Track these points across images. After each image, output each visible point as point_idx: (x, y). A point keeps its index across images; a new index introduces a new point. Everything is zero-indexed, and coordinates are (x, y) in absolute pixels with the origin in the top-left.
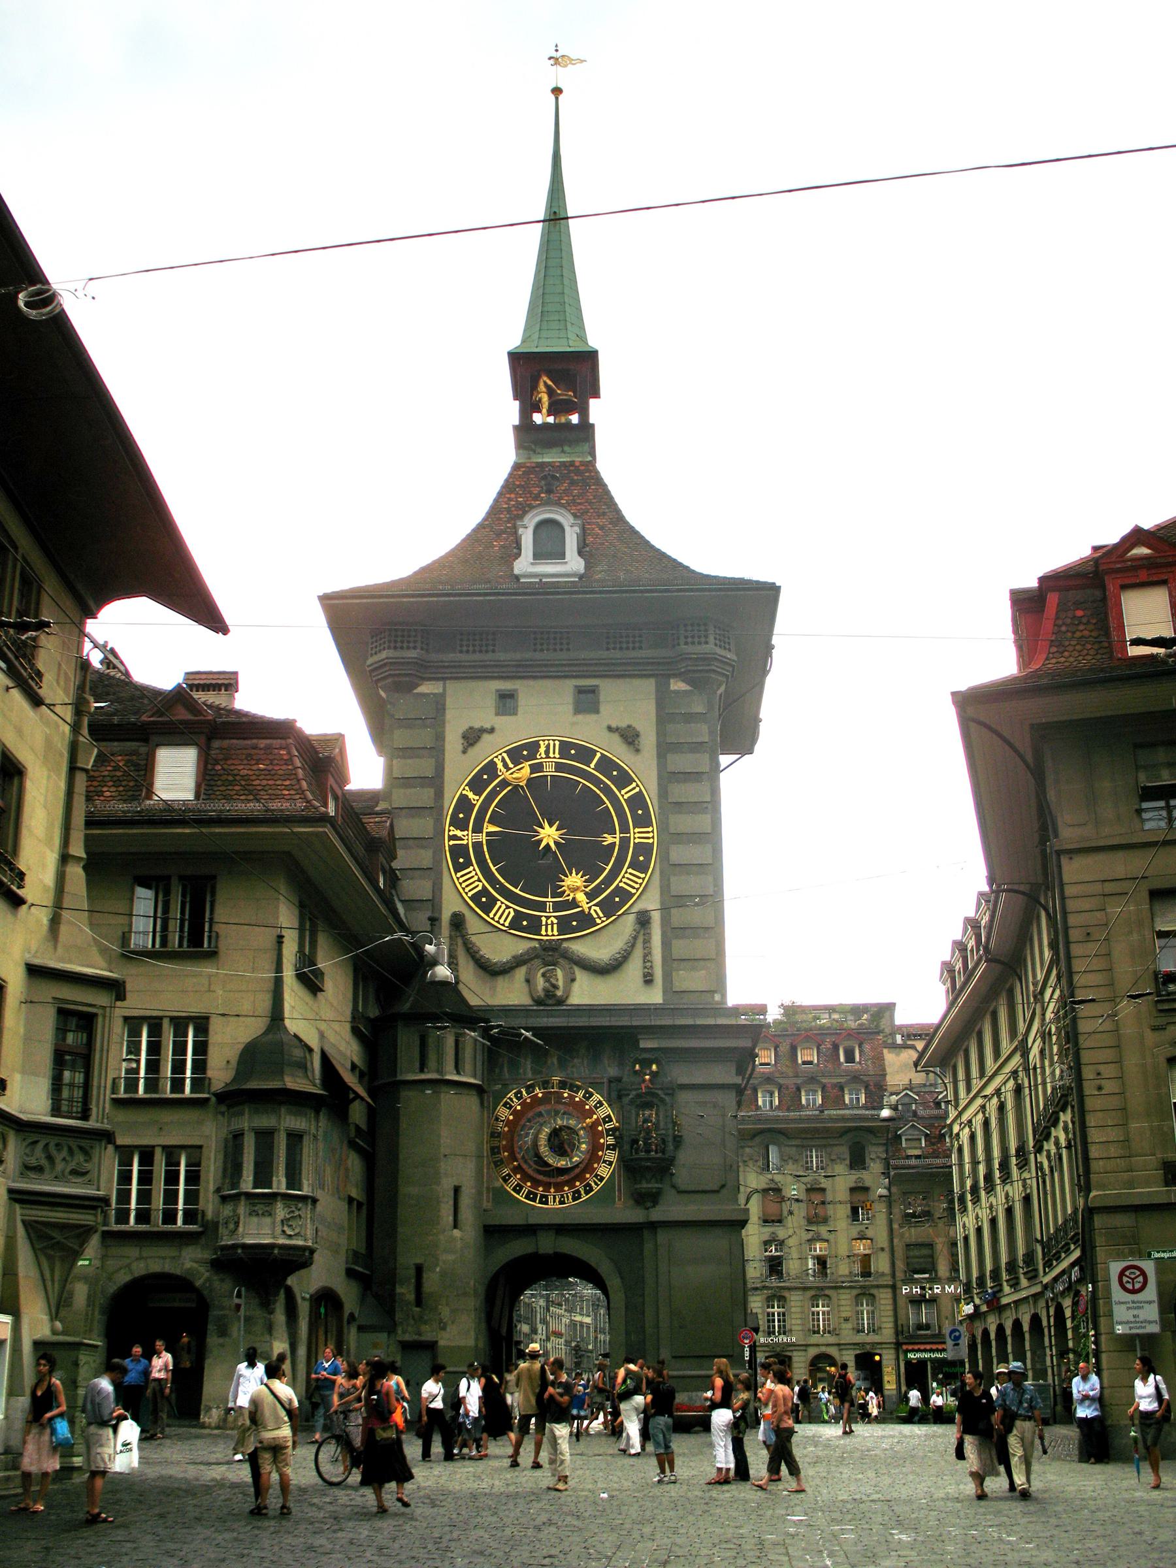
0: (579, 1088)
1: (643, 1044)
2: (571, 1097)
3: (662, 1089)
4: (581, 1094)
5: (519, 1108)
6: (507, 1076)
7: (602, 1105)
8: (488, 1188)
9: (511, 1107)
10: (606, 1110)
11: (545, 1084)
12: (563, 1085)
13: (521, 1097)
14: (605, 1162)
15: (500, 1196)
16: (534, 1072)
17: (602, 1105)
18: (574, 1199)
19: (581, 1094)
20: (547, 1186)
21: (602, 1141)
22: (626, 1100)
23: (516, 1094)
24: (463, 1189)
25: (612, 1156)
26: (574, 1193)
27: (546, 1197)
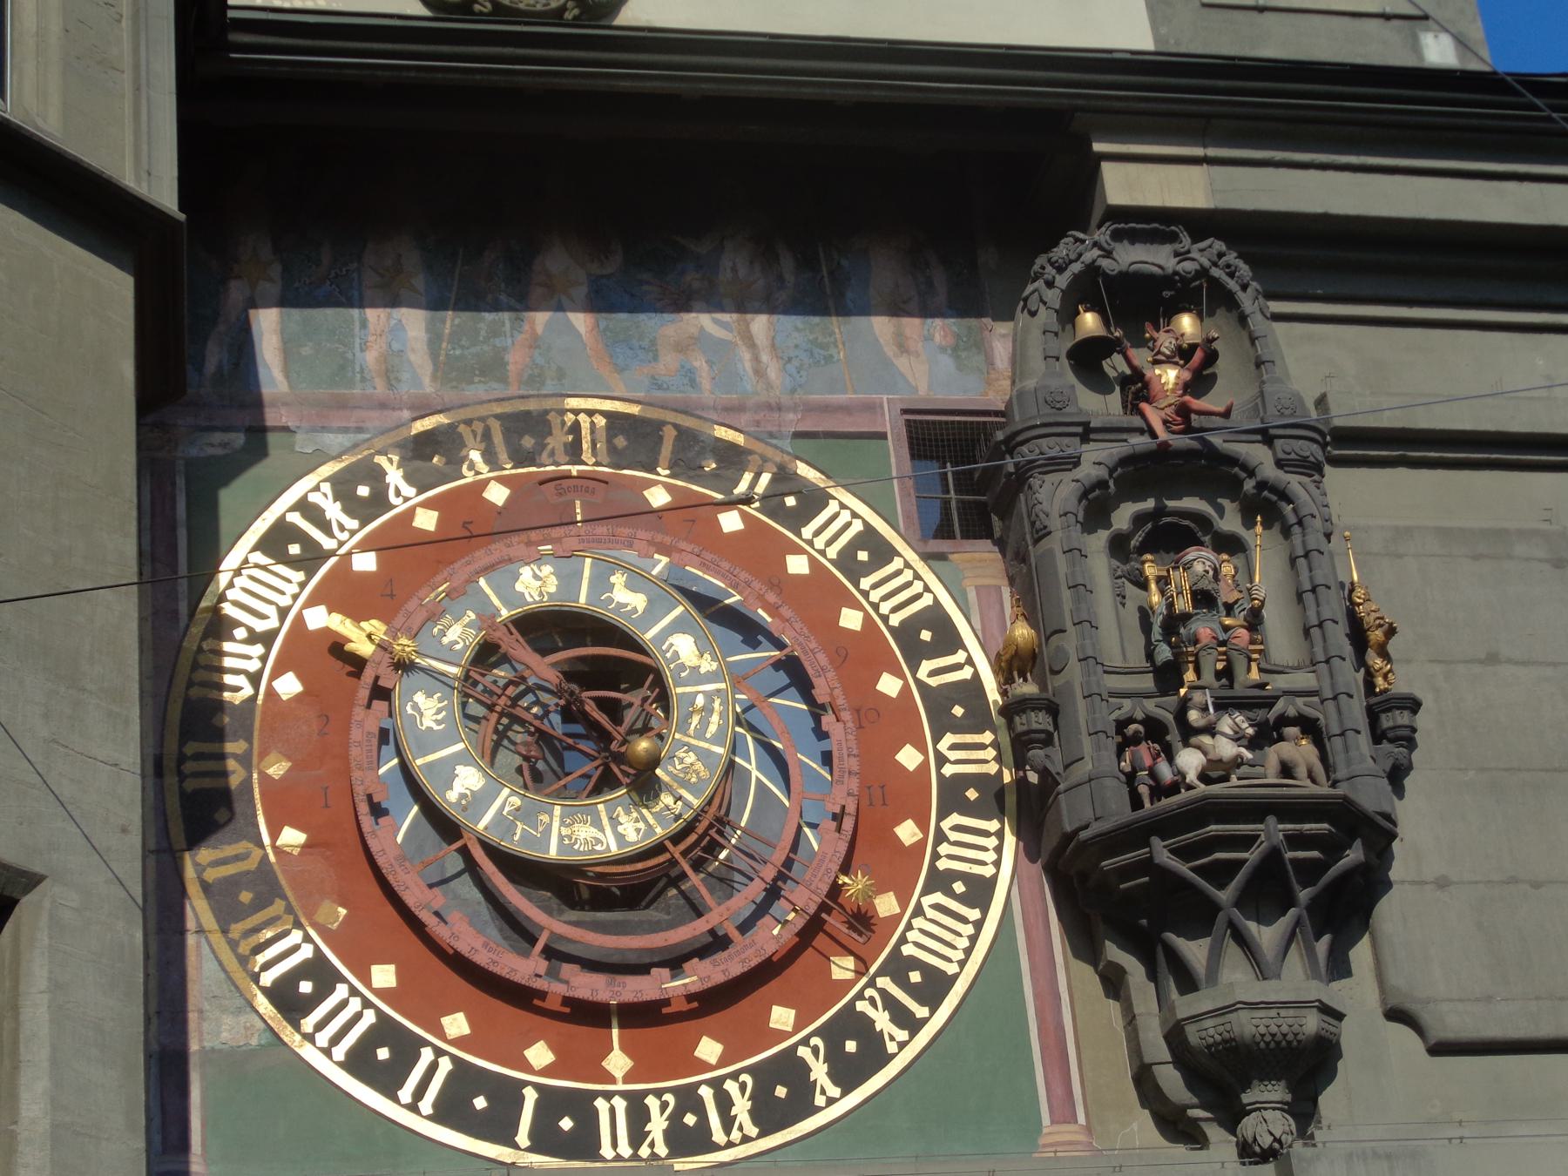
0: (733, 459)
1: (1129, 182)
2: (690, 517)
3: (1267, 438)
5: (366, 562)
7: (883, 553)
9: (312, 558)
10: (910, 583)
11: (525, 432)
12: (635, 439)
13: (379, 501)
14: (941, 880)
17: (883, 553)
18: (769, 1116)
21: (909, 757)
22: (1055, 496)
23: (342, 488)
26: (765, 1076)
27: (582, 1106)
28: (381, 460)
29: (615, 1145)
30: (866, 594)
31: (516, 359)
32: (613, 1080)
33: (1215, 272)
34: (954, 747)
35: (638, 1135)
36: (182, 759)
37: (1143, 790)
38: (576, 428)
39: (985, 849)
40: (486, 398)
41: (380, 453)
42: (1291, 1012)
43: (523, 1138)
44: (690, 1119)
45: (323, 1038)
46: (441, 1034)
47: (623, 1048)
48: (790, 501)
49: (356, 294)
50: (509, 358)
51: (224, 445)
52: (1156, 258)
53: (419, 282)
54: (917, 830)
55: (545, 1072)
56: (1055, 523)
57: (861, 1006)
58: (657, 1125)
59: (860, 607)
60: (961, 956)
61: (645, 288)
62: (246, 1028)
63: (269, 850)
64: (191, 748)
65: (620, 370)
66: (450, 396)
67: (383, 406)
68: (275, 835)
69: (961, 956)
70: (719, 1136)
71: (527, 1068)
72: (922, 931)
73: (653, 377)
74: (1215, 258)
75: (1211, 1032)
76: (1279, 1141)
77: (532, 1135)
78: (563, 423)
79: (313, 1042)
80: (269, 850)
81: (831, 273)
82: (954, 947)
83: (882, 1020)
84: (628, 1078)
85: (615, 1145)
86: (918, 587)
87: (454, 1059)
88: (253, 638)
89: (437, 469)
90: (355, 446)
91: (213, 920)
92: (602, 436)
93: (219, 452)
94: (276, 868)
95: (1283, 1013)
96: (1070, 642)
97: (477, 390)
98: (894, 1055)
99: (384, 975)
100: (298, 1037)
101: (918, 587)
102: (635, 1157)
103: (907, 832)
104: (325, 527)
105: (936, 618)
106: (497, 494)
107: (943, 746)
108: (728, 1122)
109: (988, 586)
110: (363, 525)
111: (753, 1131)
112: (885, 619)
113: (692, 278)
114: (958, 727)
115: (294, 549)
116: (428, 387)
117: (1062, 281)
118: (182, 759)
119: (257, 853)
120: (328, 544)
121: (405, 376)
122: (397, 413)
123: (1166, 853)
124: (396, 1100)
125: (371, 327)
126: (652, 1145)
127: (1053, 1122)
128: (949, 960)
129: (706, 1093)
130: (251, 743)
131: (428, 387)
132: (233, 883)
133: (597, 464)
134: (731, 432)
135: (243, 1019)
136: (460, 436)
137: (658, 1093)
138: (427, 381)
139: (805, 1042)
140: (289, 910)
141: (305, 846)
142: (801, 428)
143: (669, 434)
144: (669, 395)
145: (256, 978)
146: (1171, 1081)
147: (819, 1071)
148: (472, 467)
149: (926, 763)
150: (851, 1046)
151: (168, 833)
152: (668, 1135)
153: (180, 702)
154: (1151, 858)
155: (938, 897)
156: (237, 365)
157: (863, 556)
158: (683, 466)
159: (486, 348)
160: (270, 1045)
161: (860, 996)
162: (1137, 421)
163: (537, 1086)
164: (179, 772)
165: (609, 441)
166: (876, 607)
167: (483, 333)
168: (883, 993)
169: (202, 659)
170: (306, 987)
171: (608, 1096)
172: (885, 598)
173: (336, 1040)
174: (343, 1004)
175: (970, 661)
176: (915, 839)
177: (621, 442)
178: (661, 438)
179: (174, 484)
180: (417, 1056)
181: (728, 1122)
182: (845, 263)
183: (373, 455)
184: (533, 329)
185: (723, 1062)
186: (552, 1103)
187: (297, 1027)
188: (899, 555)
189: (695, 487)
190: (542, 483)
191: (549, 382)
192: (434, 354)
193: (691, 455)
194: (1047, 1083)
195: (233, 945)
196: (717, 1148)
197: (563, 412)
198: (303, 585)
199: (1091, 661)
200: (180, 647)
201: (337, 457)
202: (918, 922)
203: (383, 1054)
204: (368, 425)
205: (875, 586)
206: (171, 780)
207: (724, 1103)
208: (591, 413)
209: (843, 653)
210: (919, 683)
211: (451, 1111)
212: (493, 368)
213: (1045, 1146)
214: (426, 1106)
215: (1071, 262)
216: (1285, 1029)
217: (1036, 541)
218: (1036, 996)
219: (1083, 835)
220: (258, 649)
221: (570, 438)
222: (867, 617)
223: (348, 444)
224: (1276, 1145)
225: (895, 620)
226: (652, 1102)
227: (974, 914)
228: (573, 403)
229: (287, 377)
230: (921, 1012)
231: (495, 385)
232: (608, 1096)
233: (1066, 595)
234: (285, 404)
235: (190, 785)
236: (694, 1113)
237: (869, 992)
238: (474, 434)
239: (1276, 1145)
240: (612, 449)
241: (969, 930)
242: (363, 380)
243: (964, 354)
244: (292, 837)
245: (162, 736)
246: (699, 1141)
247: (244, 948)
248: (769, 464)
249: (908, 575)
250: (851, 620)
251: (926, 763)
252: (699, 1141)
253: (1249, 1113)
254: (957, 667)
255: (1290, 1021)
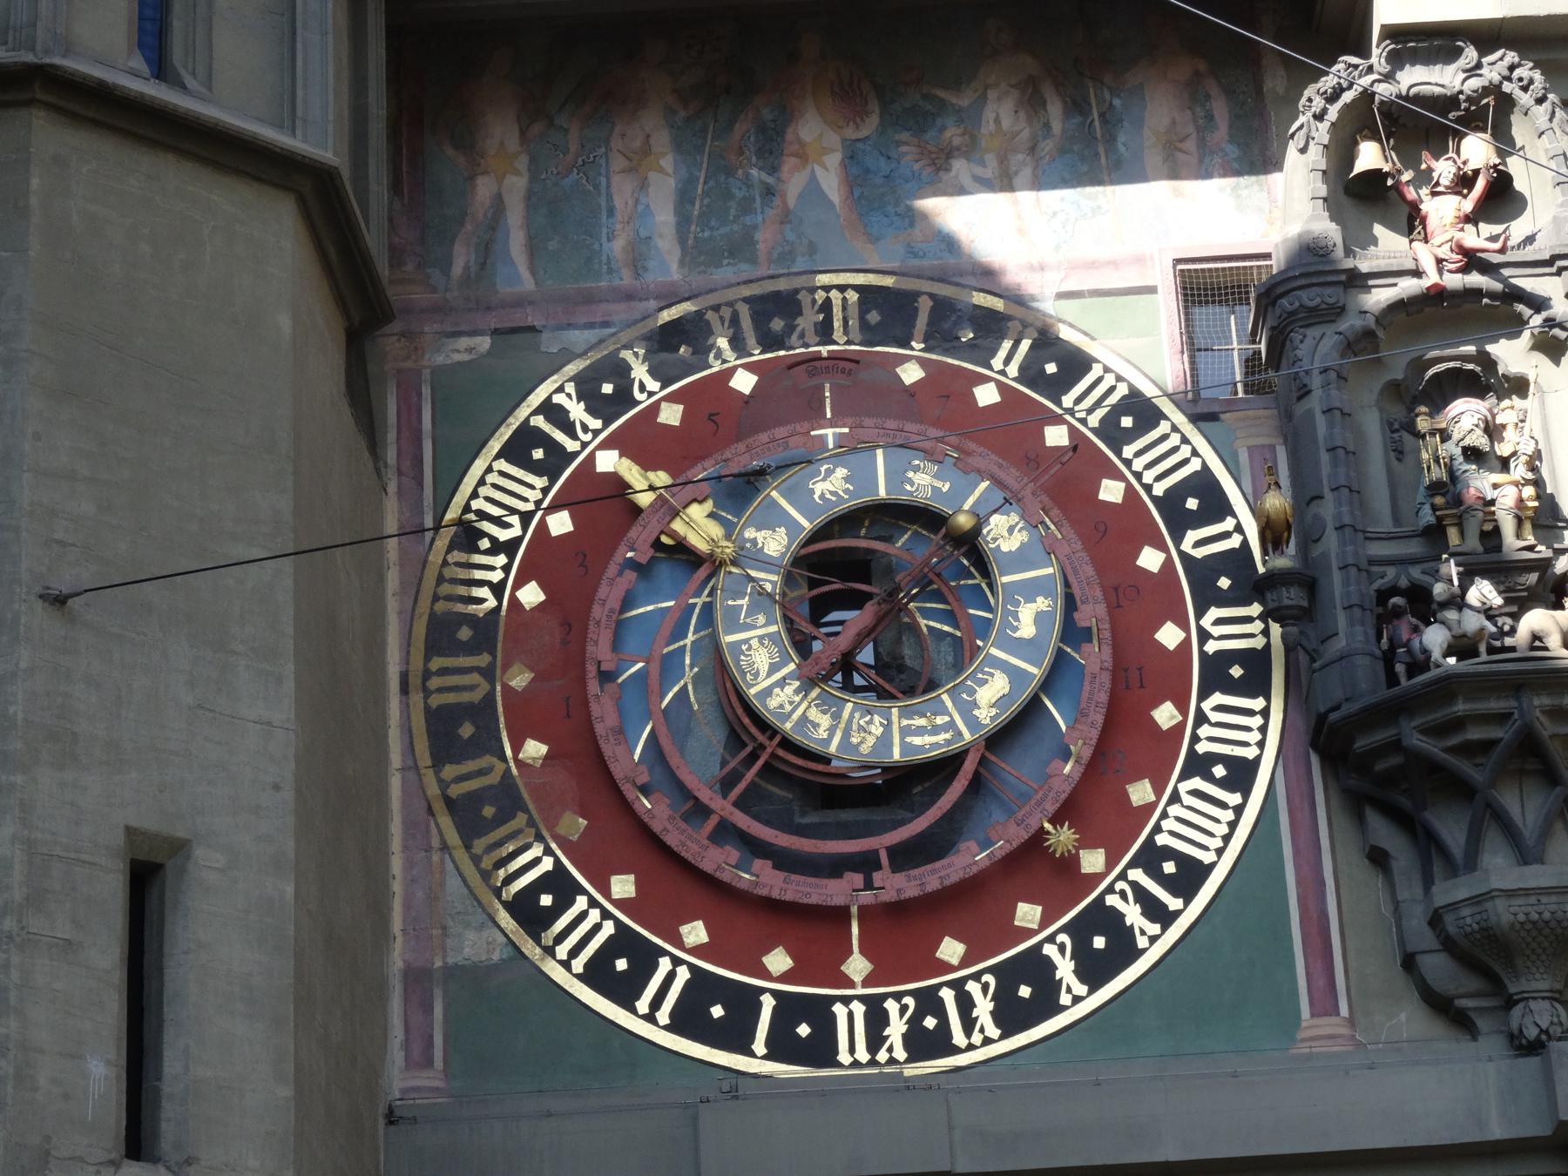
2: (947, 392)
4: (1008, 360)
6: (528, 284)
8: (418, 979)
11: (774, 313)
12: (889, 313)
13: (624, 398)
14: (1199, 765)
15: (505, 1019)
16: (697, 254)
18: (1011, 1017)
19: (1008, 360)
20: (816, 934)
21: (1169, 636)
23: (587, 390)
24: (206, 861)
25: (1254, 728)
26: (1008, 975)
27: (820, 1013)
28: (626, 355)
29: (852, 1050)
30: (1128, 463)
31: (765, 238)
32: (852, 985)
33: (1507, 87)
34: (1219, 622)
35: (876, 1040)
36: (427, 675)
37: (1400, 668)
38: (827, 304)
39: (1248, 729)
40: (736, 281)
41: (625, 347)
42: (1554, 898)
43: (759, 1047)
44: (930, 1022)
45: (562, 951)
46: (679, 944)
47: (861, 952)
48: (1051, 368)
49: (603, 181)
50: (758, 236)
51: (470, 350)
52: (1444, 78)
53: (667, 162)
54: (1176, 712)
55: (785, 978)
56: (1316, 382)
57: (1111, 900)
58: (896, 1029)
59: (1122, 478)
60: (1219, 843)
61: (904, 149)
62: (489, 943)
63: (512, 764)
64: (437, 663)
65: (874, 239)
66: (698, 281)
67: (629, 296)
68: (517, 749)
69: (1219, 843)
70: (959, 1038)
71: (765, 974)
72: (1179, 819)
73: (908, 245)
74: (1506, 73)
75: (1469, 921)
76: (1547, 1032)
77: (769, 1043)
78: (814, 301)
79: (553, 956)
80: (512, 764)
81: (1102, 115)
82: (1211, 835)
83: (1133, 914)
84: (867, 983)
85: (852, 1050)
86: (1185, 451)
87: (691, 967)
88: (497, 547)
89: (683, 361)
90: (601, 341)
91: (456, 835)
92: (854, 312)
93: (466, 357)
94: (519, 781)
95: (1544, 899)
96: (1328, 509)
97: (725, 273)
98: (1144, 951)
99: (623, 886)
100: (538, 950)
101: (1185, 451)
102: (873, 1063)
103: (1165, 715)
104: (569, 428)
105: (1204, 484)
106: (744, 382)
107: (1206, 622)
108: (969, 1024)
109: (1263, 446)
110: (605, 426)
111: (993, 1032)
112: (1148, 488)
113: (953, 134)
114: (1224, 600)
115: (538, 454)
116: (674, 273)
117: (1333, 112)
118: (427, 675)
119: (500, 766)
120: (571, 446)
121: (651, 264)
122: (644, 304)
123: (1416, 735)
124: (634, 1011)
125: (619, 216)
126: (890, 1050)
127: (1313, 1015)
128: (1206, 848)
129: (947, 995)
130: (495, 657)
131: (674, 273)
132: (476, 798)
133: (848, 343)
134: (989, 297)
135: (485, 934)
136: (708, 323)
137: (898, 996)
138: (674, 267)
139: (1051, 939)
140: (531, 823)
141: (547, 757)
142: (1066, 288)
143: (925, 305)
144: (925, 263)
145: (498, 892)
146: (1437, 967)
147: (1065, 969)
148: (719, 355)
149: (1187, 641)
150: (1099, 942)
151: (413, 750)
152: (906, 1038)
153: (425, 618)
154: (1399, 740)
155: (1197, 783)
156: (483, 265)
157: (1127, 422)
158: (941, 337)
159: (735, 227)
160: (511, 959)
161: (1110, 890)
162: (1410, 265)
163: (775, 994)
164: (425, 689)
165: (862, 318)
166: (1138, 476)
167: (733, 212)
168: (1135, 886)
169: (448, 573)
170: (546, 900)
171: (846, 1001)
172: (1149, 466)
173: (575, 952)
174: (582, 916)
175: (1239, 529)
176: (1174, 722)
177: (874, 317)
178: (916, 310)
179: (420, 394)
180: (655, 966)
181: (969, 1024)
182: (1117, 102)
183: (618, 350)
184: (785, 203)
185: (965, 963)
186: (789, 1009)
187: (537, 941)
188: (1167, 418)
189: (950, 361)
190: (790, 367)
191: (799, 259)
192: (682, 239)
193: (946, 325)
194: (1308, 974)
195: (476, 860)
196: (957, 1050)
197: (813, 290)
198: (545, 491)
199: (1348, 531)
200: (425, 562)
201: (580, 356)
202: (1174, 810)
203: (622, 965)
204: (615, 318)
205: (1138, 454)
206: (416, 698)
207: (966, 1004)
208: (842, 288)
209: (1102, 528)
210: (1184, 557)
211: (687, 1021)
212: (741, 248)
213: (1303, 1040)
214: (663, 1016)
215: (1342, 90)
216: (1547, 916)
217: (1300, 398)
218: (1299, 883)
219: (1333, 716)
220: (501, 560)
221: (821, 317)
222: (1129, 489)
223: (594, 340)
224: (1544, 1037)
225: (1159, 489)
226: (891, 1006)
227: (1234, 799)
228: (823, 279)
229: (533, 273)
230: (1174, 903)
231: (744, 266)
232: (846, 1001)
233: (1325, 457)
234: (530, 303)
235: (436, 701)
236: (934, 1016)
237: (1120, 885)
238: (722, 319)
239: (1544, 1037)
240: (864, 325)
241: (1229, 815)
242: (610, 271)
243: (1245, 193)
244: (535, 749)
245: (408, 652)
246: (939, 1044)
247: (487, 863)
248: (1028, 331)
249: (1175, 440)
250: (1111, 491)
251: (1187, 641)
252: (939, 1044)
253: (1517, 1002)
254: (1225, 535)
255: (1553, 907)
